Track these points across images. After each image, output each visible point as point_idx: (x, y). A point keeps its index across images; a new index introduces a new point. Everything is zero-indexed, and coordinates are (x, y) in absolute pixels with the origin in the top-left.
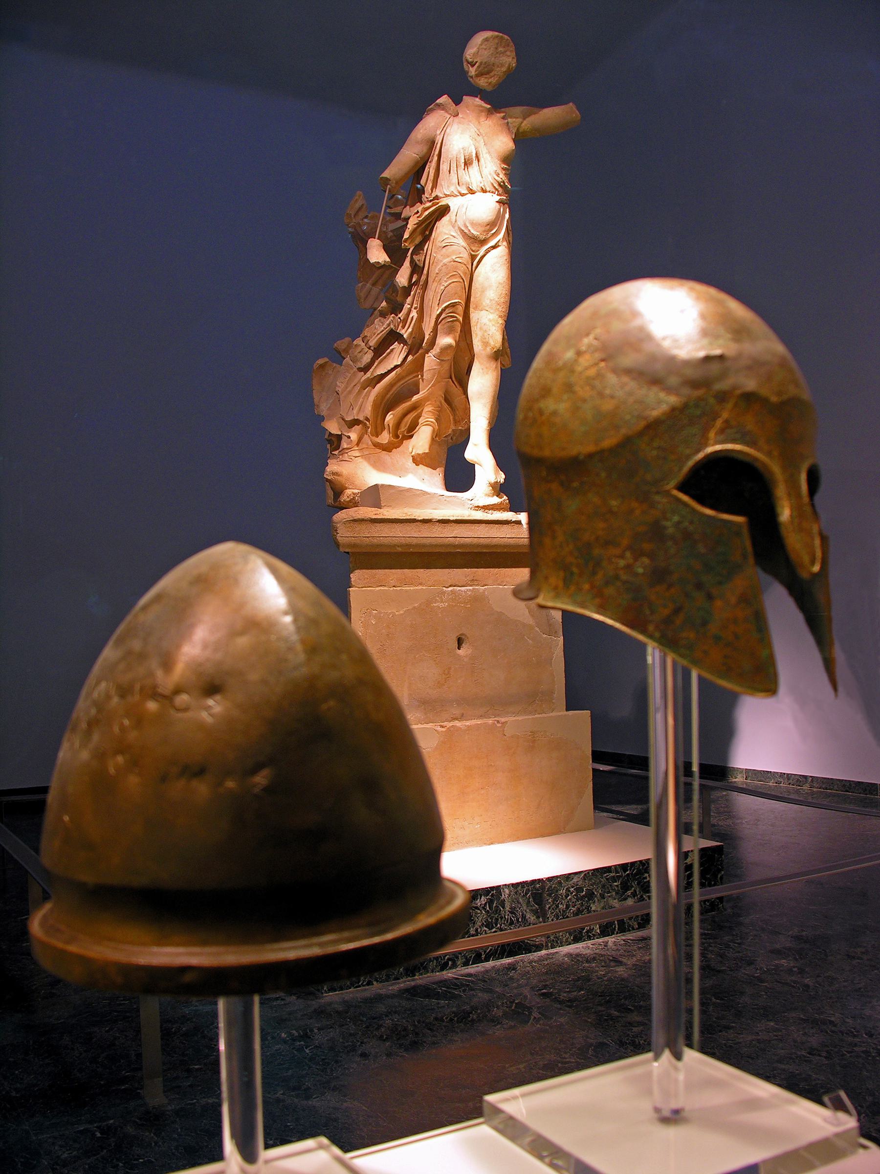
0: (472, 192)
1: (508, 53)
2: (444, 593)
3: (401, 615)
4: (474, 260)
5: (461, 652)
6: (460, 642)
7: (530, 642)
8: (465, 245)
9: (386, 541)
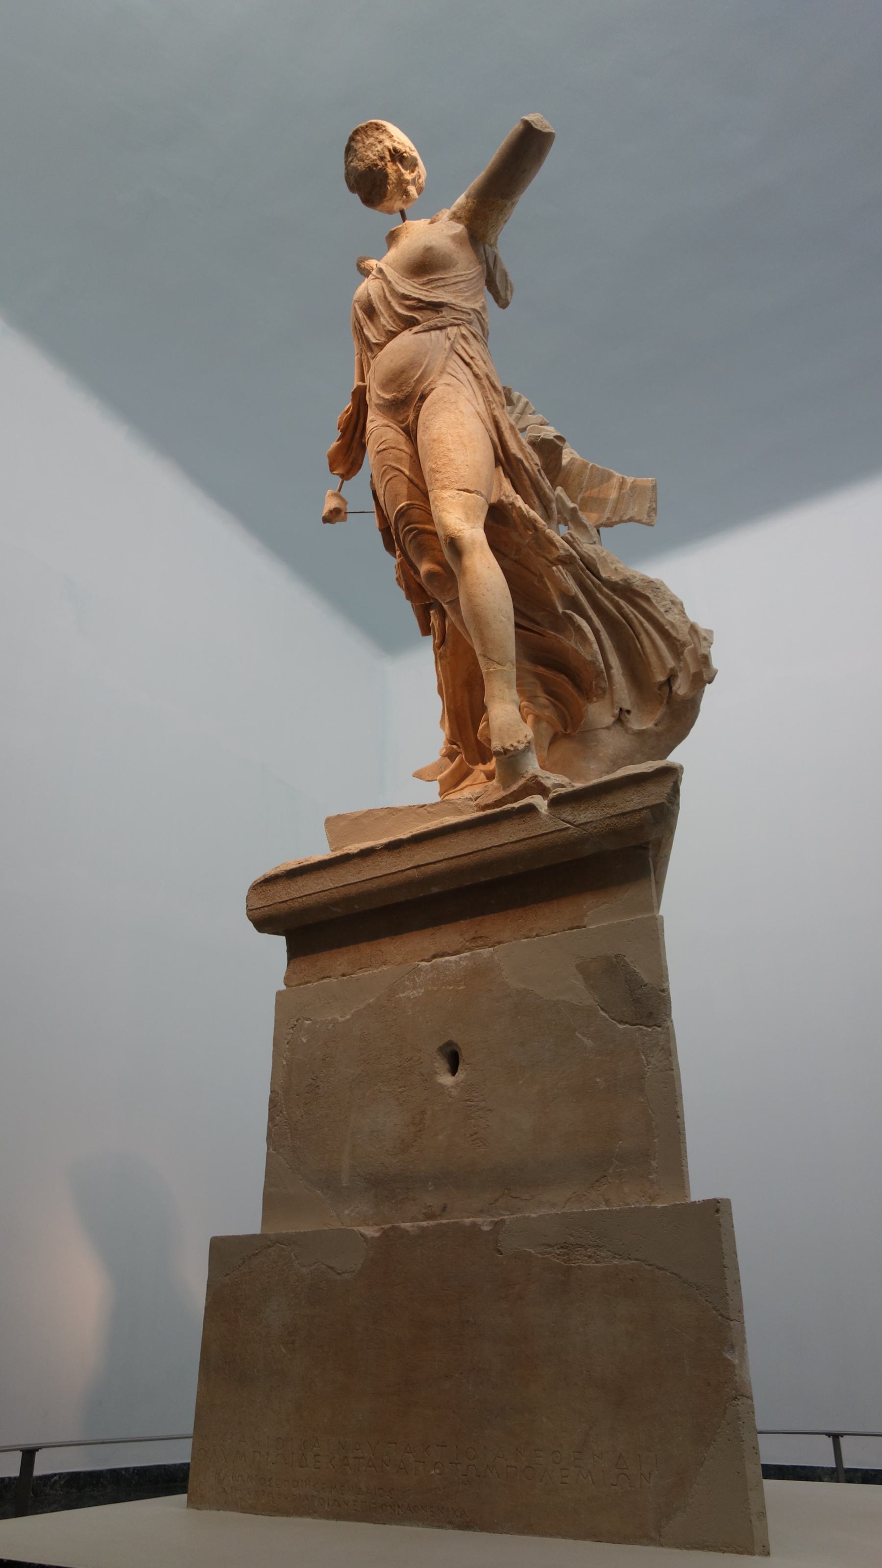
0: (381, 346)
1: (382, 137)
2: (417, 970)
3: (348, 1021)
4: (411, 433)
5: (447, 1080)
6: (454, 1061)
7: (589, 1043)
8: (386, 422)
9: (310, 901)
